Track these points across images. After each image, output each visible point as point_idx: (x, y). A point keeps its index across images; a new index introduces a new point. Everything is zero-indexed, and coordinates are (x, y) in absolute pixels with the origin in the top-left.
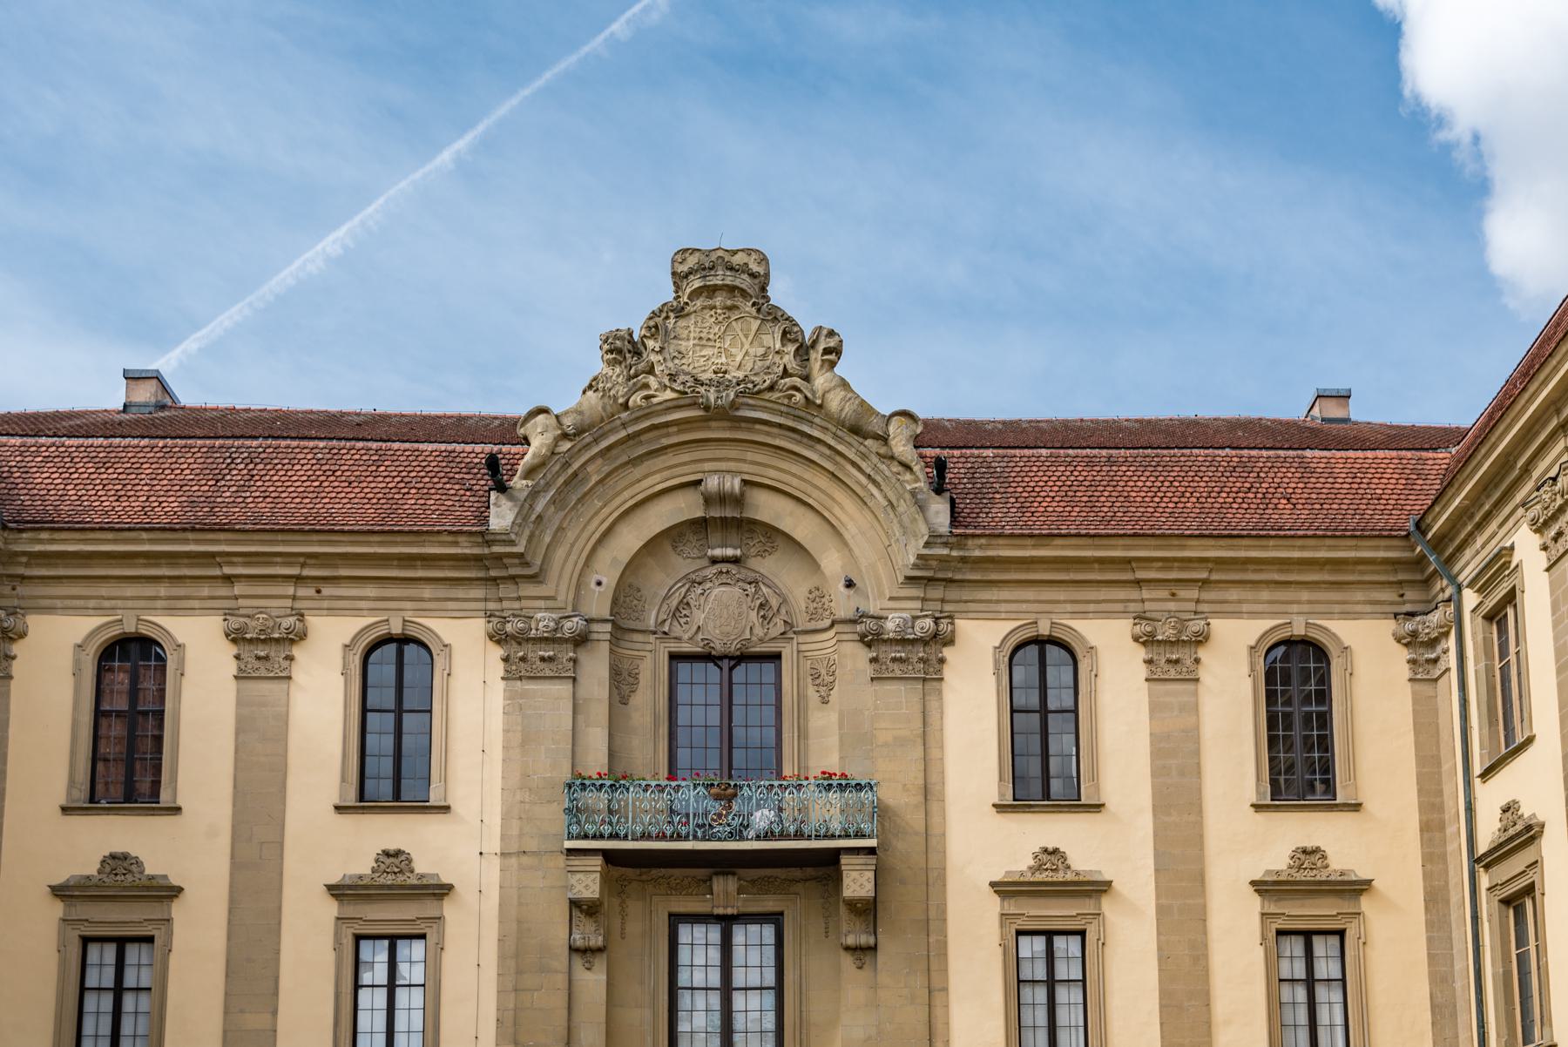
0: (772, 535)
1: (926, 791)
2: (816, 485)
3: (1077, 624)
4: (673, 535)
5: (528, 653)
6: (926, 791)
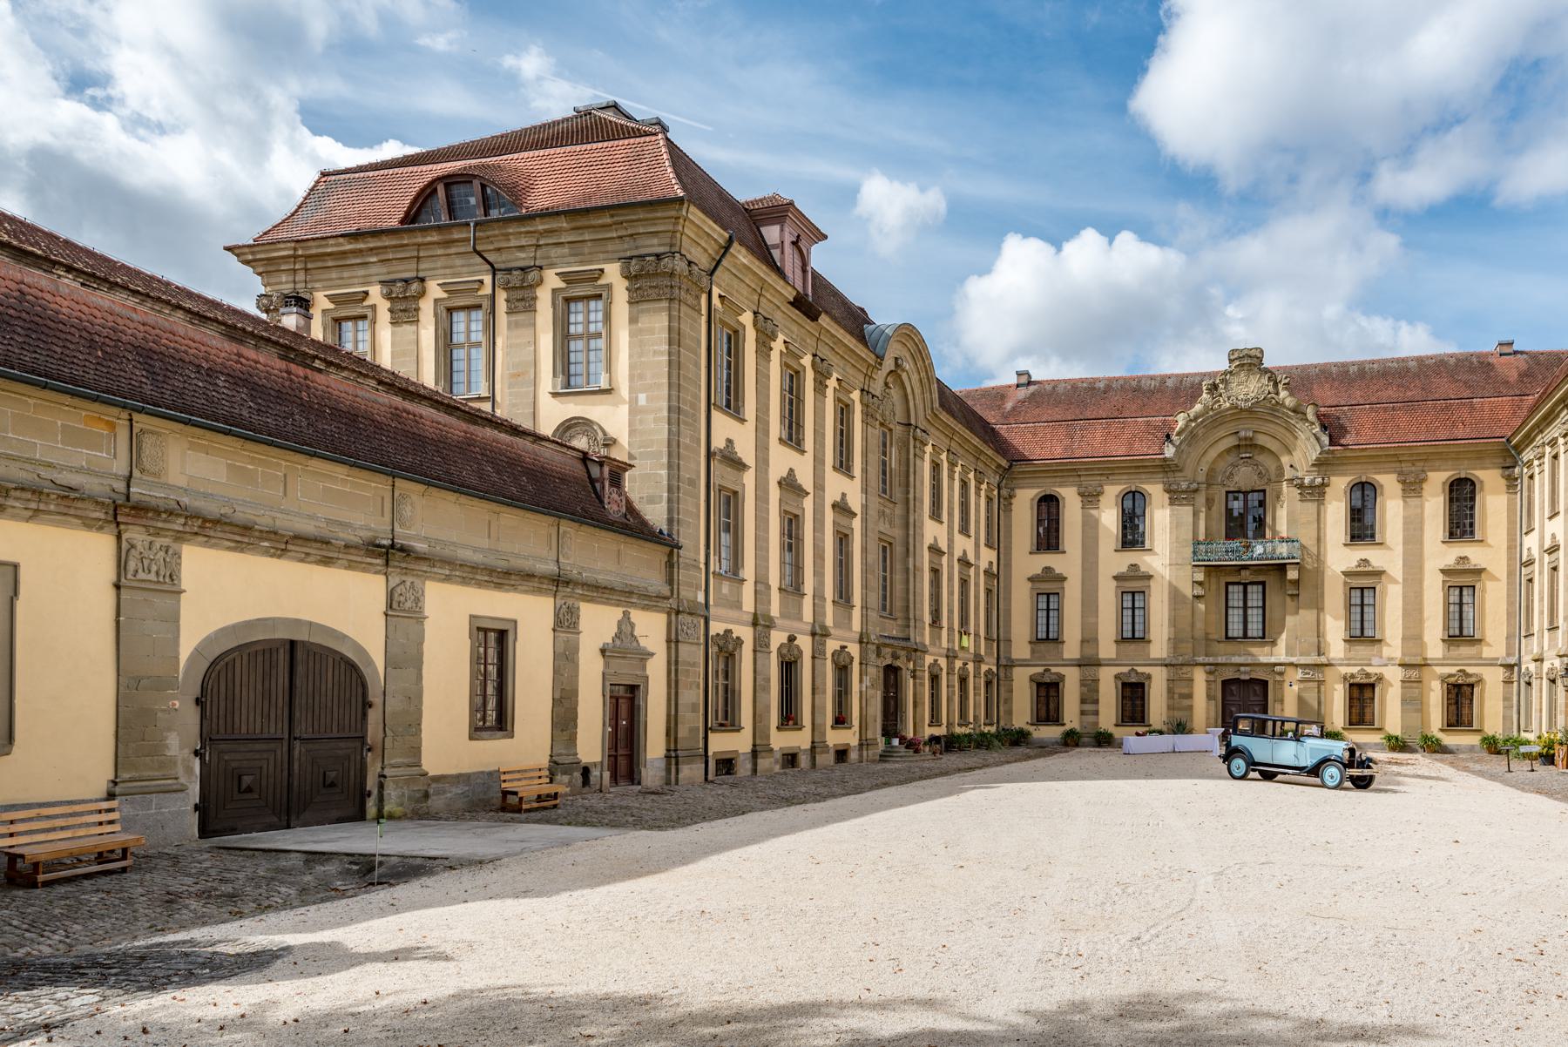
0: (1263, 449)
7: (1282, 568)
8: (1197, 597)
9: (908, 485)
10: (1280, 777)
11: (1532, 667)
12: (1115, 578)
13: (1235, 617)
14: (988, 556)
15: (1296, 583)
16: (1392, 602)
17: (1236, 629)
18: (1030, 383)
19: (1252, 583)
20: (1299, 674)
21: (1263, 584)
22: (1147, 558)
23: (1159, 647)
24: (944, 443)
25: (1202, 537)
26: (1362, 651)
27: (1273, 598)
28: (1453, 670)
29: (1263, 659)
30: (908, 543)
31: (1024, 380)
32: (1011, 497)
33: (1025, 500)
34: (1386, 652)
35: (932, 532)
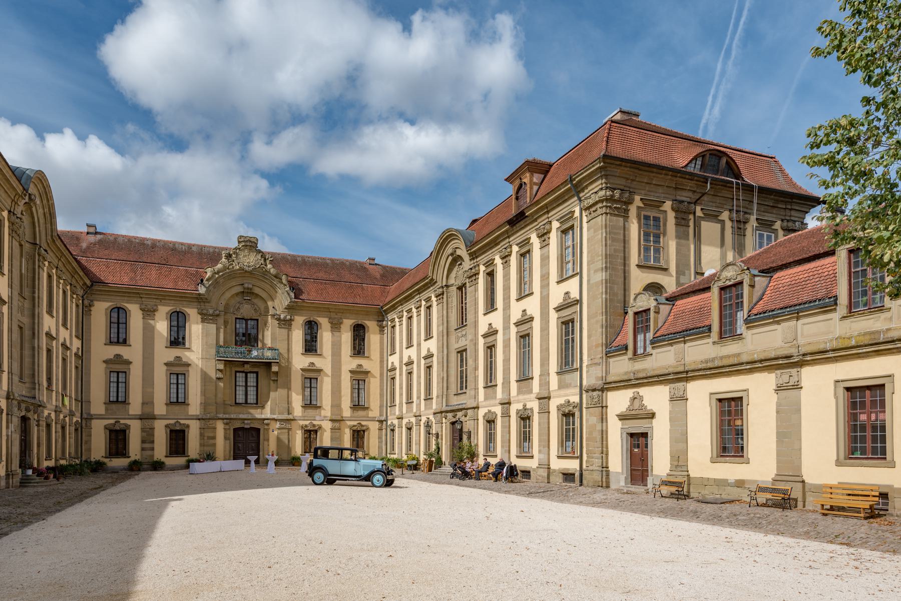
1: (288, 350)
2: (267, 287)
3: (318, 319)
4: (237, 294)
5: (205, 318)
6: (288, 350)
7: (268, 365)
8: (219, 379)
9: (34, 287)
10: (337, 482)
11: (396, 422)
12: (166, 364)
13: (240, 392)
14: (76, 344)
15: (276, 373)
16: (326, 386)
17: (241, 398)
18: (96, 233)
19: (250, 372)
20: (278, 425)
21: (257, 373)
22: (187, 353)
23: (195, 406)
24: (55, 261)
25: (221, 343)
26: (311, 412)
27: (263, 382)
28: (355, 423)
29: (258, 416)
30: (33, 329)
31: (92, 230)
32: (90, 306)
33: (100, 309)
34: (323, 413)
35: (48, 323)
